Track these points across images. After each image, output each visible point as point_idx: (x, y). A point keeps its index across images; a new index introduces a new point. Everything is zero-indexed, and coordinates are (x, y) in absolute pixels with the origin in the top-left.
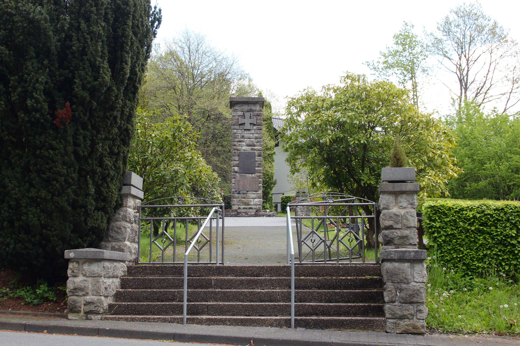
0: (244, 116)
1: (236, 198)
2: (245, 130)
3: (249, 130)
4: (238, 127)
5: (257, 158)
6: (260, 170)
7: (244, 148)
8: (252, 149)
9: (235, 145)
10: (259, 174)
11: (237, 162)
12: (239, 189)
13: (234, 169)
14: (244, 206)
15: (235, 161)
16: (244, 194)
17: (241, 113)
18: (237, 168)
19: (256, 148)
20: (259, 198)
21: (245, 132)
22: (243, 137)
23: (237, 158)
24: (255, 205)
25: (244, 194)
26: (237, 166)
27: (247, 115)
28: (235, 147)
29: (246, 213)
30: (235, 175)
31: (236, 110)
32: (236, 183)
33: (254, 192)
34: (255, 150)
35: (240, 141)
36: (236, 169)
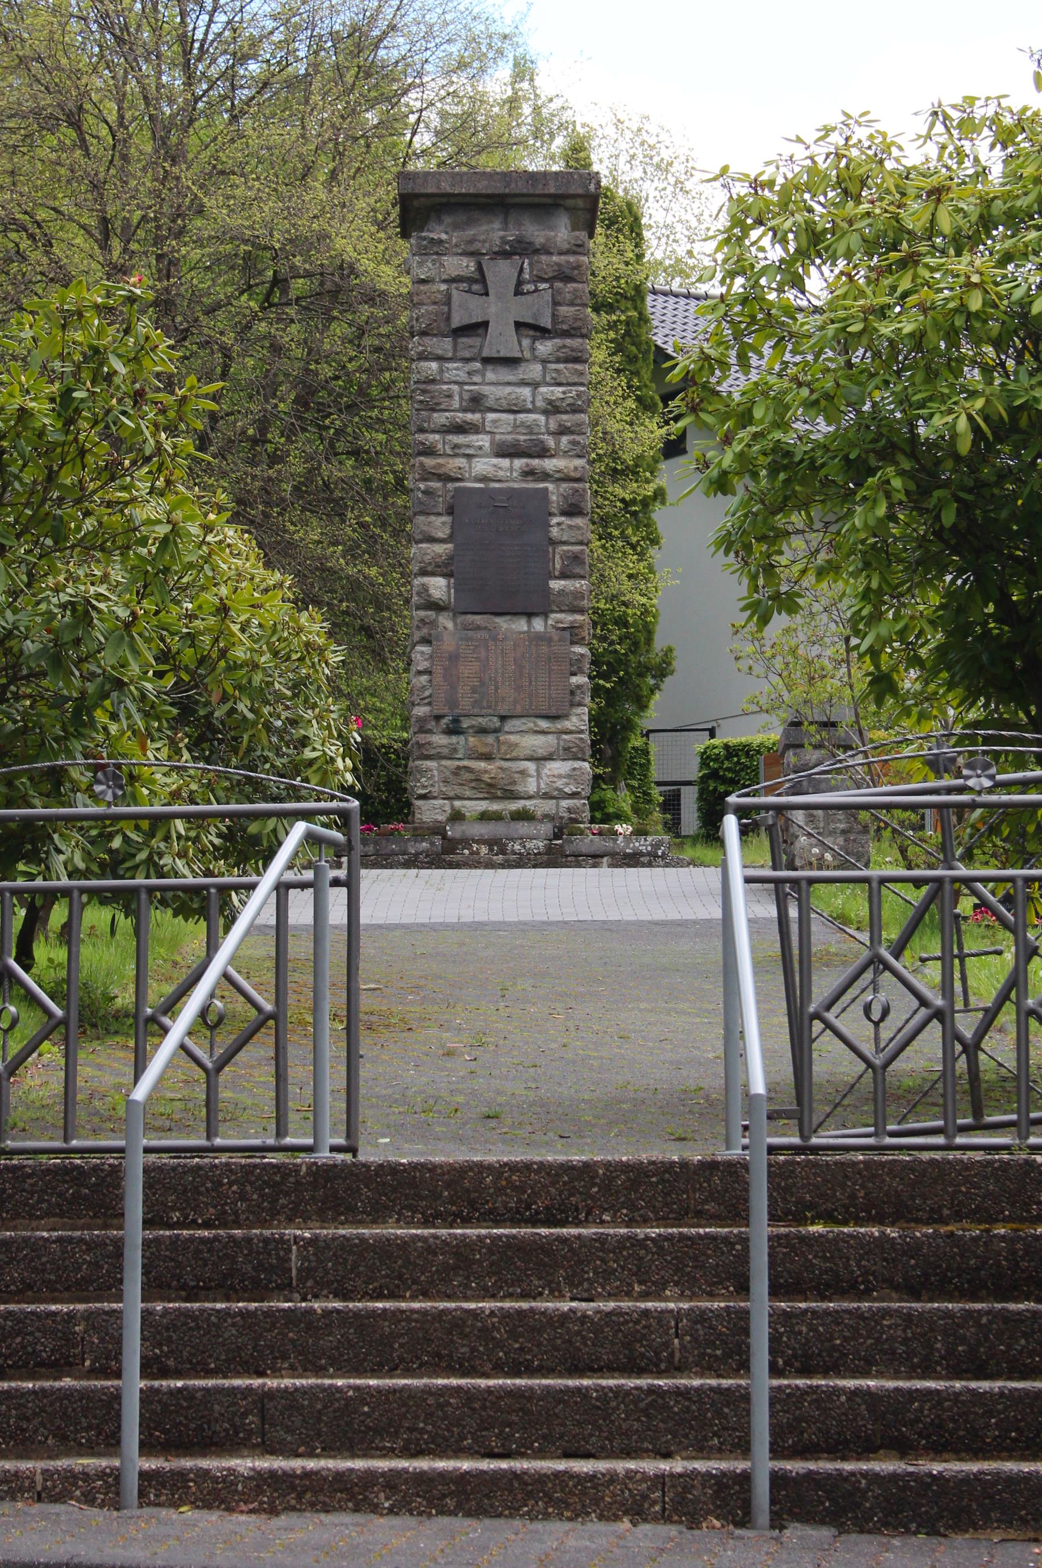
1: (439, 757)
2: (487, 361)
3: (511, 362)
4: (444, 345)
5: (559, 526)
6: (578, 595)
7: (483, 466)
8: (529, 473)
9: (429, 451)
10: (569, 618)
11: (440, 549)
12: (453, 703)
13: (425, 588)
14: (483, 806)
16: (483, 731)
19: (550, 464)
20: (569, 753)
21: (490, 376)
22: (476, 402)
23: (440, 525)
24: (547, 796)
25: (483, 731)
26: (443, 568)
27: (502, 273)
28: (429, 462)
29: (496, 844)
30: (433, 624)
31: (434, 249)
32: (438, 670)
33: (544, 724)
34: (546, 476)
35: (461, 429)
36: (438, 586)
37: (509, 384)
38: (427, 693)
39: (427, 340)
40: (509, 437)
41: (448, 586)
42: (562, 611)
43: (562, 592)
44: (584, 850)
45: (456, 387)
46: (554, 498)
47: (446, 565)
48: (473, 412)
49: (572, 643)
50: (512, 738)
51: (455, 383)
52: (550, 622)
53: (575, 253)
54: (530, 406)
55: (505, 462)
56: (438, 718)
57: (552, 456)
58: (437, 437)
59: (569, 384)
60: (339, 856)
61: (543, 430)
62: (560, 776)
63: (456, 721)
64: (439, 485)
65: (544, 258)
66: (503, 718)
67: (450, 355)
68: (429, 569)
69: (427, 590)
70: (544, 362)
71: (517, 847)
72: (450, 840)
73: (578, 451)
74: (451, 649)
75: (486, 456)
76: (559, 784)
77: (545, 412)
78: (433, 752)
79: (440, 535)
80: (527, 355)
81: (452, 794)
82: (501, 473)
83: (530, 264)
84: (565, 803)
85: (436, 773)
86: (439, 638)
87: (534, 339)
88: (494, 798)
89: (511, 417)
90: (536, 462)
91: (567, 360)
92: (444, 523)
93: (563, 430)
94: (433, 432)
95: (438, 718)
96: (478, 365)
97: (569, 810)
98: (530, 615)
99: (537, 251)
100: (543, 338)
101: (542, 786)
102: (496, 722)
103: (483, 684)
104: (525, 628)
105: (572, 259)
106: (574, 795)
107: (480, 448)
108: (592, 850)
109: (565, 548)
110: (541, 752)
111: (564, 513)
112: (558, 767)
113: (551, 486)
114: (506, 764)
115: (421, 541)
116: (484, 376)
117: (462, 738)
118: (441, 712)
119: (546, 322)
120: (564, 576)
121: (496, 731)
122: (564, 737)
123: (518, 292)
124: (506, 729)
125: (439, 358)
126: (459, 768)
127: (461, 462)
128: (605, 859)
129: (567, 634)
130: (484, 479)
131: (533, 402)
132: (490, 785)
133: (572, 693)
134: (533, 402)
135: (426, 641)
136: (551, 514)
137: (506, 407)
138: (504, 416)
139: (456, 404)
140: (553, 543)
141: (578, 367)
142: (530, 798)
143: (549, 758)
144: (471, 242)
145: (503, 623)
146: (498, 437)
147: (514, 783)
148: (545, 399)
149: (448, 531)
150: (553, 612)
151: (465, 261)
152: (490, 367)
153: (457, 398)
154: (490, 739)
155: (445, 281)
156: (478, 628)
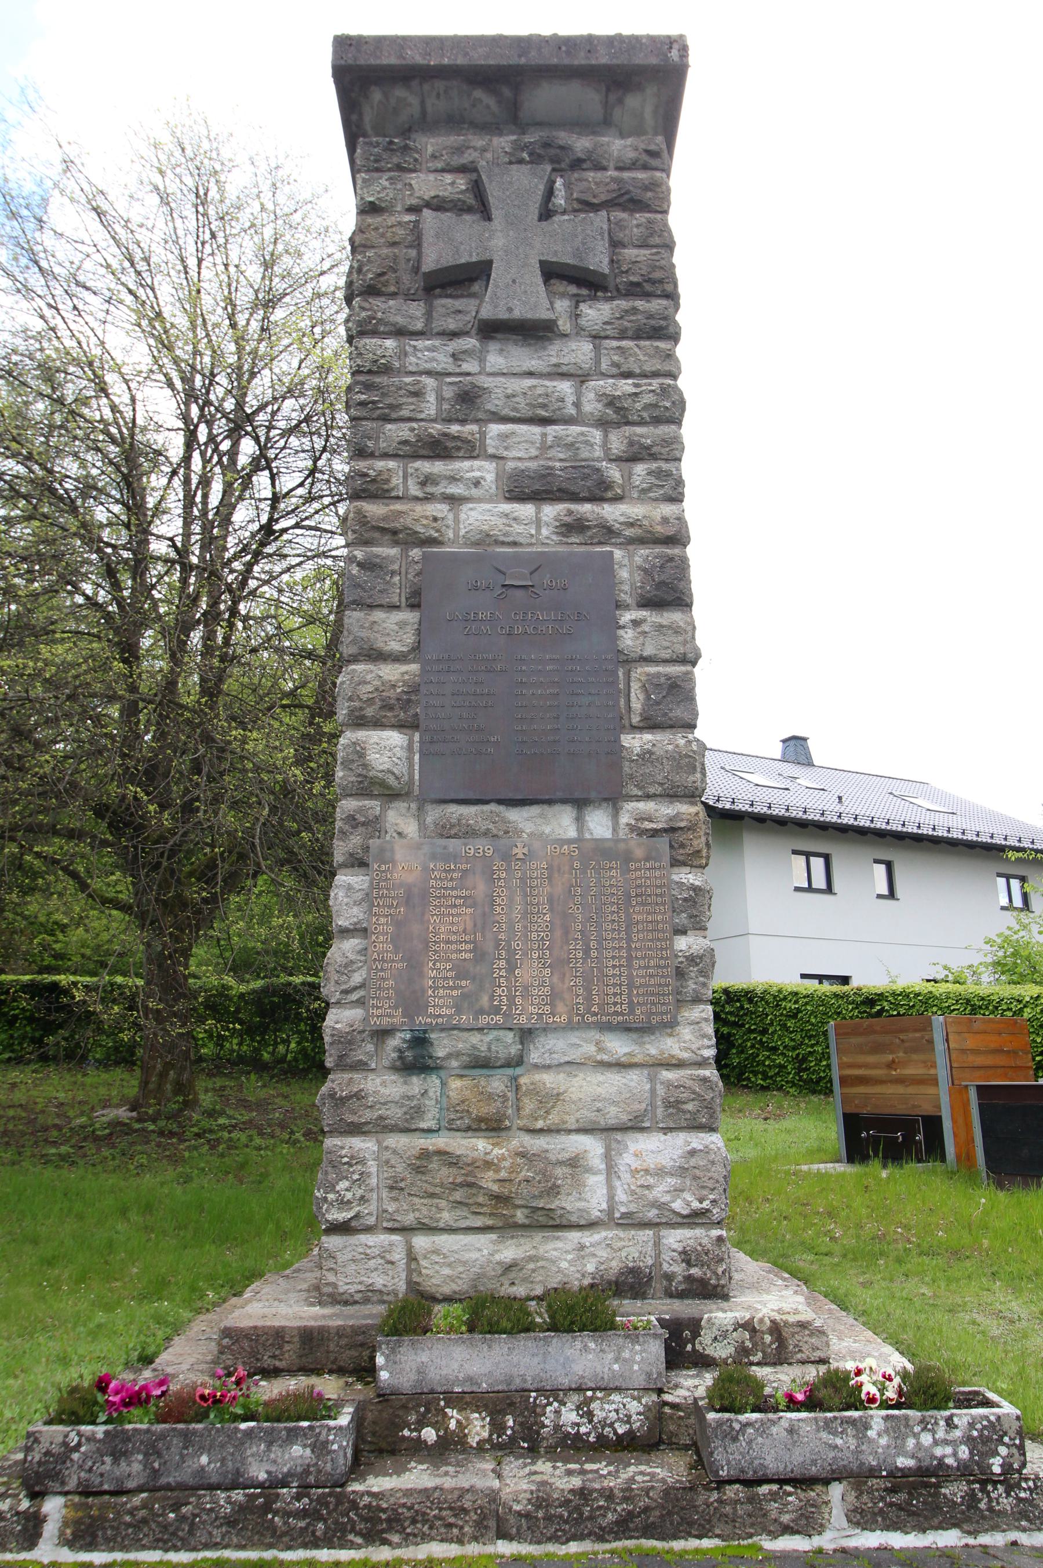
0: (478, 204)
1: (382, 1127)
4: (414, 313)
7: (483, 515)
10: (664, 811)
11: (390, 672)
12: (412, 1002)
13: (359, 752)
15: (377, 656)
16: (481, 1063)
17: (455, 185)
18: (394, 738)
19: (612, 513)
21: (495, 360)
22: (468, 400)
24: (631, 1222)
25: (481, 1063)
26: (397, 711)
30: (374, 825)
33: (619, 1046)
34: (608, 532)
35: (439, 449)
37: (530, 374)
38: (357, 978)
39: (377, 302)
40: (533, 465)
41: (410, 748)
42: (648, 797)
43: (647, 756)
44: (773, 1461)
45: (430, 382)
46: (624, 574)
47: (405, 703)
48: (463, 422)
49: (675, 863)
50: (549, 1080)
51: (429, 373)
52: (624, 819)
53: (645, 167)
54: (573, 411)
55: (527, 510)
56: (382, 1034)
57: (618, 499)
58: (391, 464)
59: (644, 375)
60: (37, 1495)
61: (598, 453)
62: (661, 1172)
63: (420, 1041)
64: (393, 551)
65: (591, 175)
66: (526, 1035)
67: (419, 326)
68: (369, 712)
69: (362, 755)
70: (596, 337)
71: (569, 1416)
72: (384, 1397)
73: (668, 490)
74: (410, 878)
75: (490, 500)
76: (660, 1191)
77: (603, 424)
78: (368, 1115)
79: (394, 646)
80: (564, 325)
81: (409, 1219)
82: (518, 528)
83: (568, 186)
84: (675, 1238)
85: (372, 1167)
86: (385, 857)
87: (577, 300)
88: (507, 1228)
89: (537, 430)
90: (586, 508)
91: (637, 336)
92: (402, 625)
93: (635, 455)
94: (385, 456)
95: (382, 1034)
96: (470, 342)
97: (687, 1257)
98: (580, 804)
99: (577, 164)
100: (595, 298)
101: (621, 1196)
102: (508, 1044)
103: (480, 955)
104: (572, 833)
105: (641, 175)
106: (695, 1218)
107: (477, 483)
108: (795, 1460)
109: (652, 669)
110: (614, 1114)
111: (648, 603)
112: (657, 1149)
113: (618, 554)
114: (539, 1143)
115: (354, 659)
116: (482, 361)
117: (434, 1082)
118: (385, 1022)
119: (599, 261)
120: (650, 724)
121: (517, 1061)
123: (546, 213)
124: (534, 1056)
125: (400, 332)
126: (425, 1155)
127: (440, 509)
128: (836, 1490)
129: (662, 843)
130: (485, 539)
131: (577, 405)
132: (499, 1199)
133: (680, 974)
134: (577, 405)
135: (358, 862)
136: (619, 606)
137: (526, 412)
138: (523, 428)
139: (430, 406)
140: (629, 661)
141: (662, 345)
142: (592, 1225)
143: (635, 1126)
144: (459, 150)
145: (524, 820)
146: (511, 465)
147: (554, 1191)
148: (601, 396)
149: (410, 639)
151: (448, 178)
152: (493, 346)
153: (431, 398)
154: (497, 1083)
155: (411, 209)
156: (470, 833)
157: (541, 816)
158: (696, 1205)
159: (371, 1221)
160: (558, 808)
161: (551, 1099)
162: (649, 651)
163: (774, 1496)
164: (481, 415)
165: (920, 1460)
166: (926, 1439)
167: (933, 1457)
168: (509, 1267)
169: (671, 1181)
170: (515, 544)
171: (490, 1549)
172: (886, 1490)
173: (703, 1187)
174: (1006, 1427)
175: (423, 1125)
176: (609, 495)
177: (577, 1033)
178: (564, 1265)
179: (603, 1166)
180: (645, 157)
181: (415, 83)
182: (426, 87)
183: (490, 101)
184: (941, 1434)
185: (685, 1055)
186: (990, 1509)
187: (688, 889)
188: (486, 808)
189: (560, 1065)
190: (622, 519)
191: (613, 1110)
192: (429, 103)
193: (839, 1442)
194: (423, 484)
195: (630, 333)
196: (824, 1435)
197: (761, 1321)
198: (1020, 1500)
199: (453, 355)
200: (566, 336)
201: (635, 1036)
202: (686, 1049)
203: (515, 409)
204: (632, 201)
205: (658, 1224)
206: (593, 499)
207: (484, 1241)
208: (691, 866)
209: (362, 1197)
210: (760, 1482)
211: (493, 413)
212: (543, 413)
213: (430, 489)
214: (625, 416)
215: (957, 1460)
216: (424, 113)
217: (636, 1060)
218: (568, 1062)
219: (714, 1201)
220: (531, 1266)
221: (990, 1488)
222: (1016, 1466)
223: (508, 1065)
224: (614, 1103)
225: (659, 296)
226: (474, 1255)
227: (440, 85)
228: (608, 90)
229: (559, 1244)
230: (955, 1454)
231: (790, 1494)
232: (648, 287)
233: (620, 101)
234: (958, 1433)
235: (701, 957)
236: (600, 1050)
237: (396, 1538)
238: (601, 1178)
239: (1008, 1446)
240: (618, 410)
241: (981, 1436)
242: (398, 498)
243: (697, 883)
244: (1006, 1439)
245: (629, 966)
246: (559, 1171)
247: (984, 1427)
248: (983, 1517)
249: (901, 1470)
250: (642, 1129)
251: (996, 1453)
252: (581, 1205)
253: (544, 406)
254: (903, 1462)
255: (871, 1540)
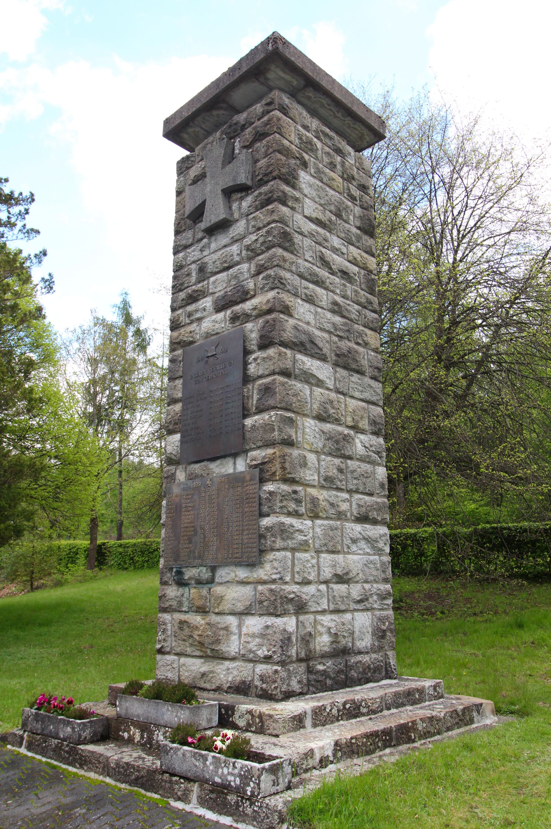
16: (199, 582)
37: (225, 246)
42: (259, 447)
62: (253, 636)
75: (211, 314)
76: (252, 646)
84: (261, 668)
89: (224, 274)
90: (237, 308)
97: (262, 678)
106: (267, 659)
109: (261, 382)
114: (218, 619)
120: (260, 411)
122: (260, 588)
133: (262, 536)
137: (221, 268)
142: (233, 659)
143: (247, 612)
150: (252, 449)
157: (221, 464)
158: (266, 653)
159: (168, 649)
160: (225, 461)
161: (221, 598)
162: (260, 372)
163: (177, 783)
164: (208, 275)
165: (222, 780)
166: (225, 771)
167: (227, 780)
168: (203, 675)
169: (257, 640)
170: (217, 334)
171: (104, 779)
172: (210, 790)
173: (271, 644)
174: (254, 773)
175: (184, 609)
176: (249, 296)
177: (227, 568)
178: (222, 676)
179: (237, 631)
180: (266, 108)
181: (191, 124)
182: (196, 122)
183: (221, 112)
184: (230, 770)
185: (266, 578)
186: (243, 811)
187: (268, 493)
188: (202, 464)
189: (226, 582)
190: (251, 307)
191: (239, 604)
192: (203, 126)
193: (197, 764)
194: (189, 317)
195: (259, 207)
196: (193, 759)
197: (256, 711)
198: (254, 811)
199: (200, 250)
200: (237, 220)
201: (249, 568)
202: (266, 575)
203: (217, 268)
204: (261, 135)
205: (256, 661)
206: (243, 301)
207: (198, 661)
208: (273, 481)
209: (164, 639)
210: (175, 775)
211: (211, 272)
212: (226, 265)
213: (191, 318)
214: (256, 253)
215: (235, 784)
216: (206, 130)
217: (250, 580)
218: (228, 582)
219: (274, 652)
220: (211, 675)
221: (244, 801)
222: (256, 793)
223: (208, 583)
224: (240, 601)
225: (271, 180)
226: (194, 668)
227: (199, 119)
228: (257, 79)
229: (221, 667)
230: (235, 781)
231: (182, 783)
232: (265, 179)
233: (267, 79)
234: (236, 771)
235: (272, 527)
236: (236, 576)
237: (86, 768)
238: (236, 637)
239: (254, 783)
240: (252, 251)
241: (244, 774)
242: (183, 326)
243: (272, 489)
244: (253, 779)
245: (242, 534)
246: (222, 632)
247: (246, 771)
248: (240, 815)
249: (216, 783)
250: (253, 614)
251: (249, 785)
252: (228, 649)
253: (225, 262)
254: (217, 780)
255: (201, 811)
